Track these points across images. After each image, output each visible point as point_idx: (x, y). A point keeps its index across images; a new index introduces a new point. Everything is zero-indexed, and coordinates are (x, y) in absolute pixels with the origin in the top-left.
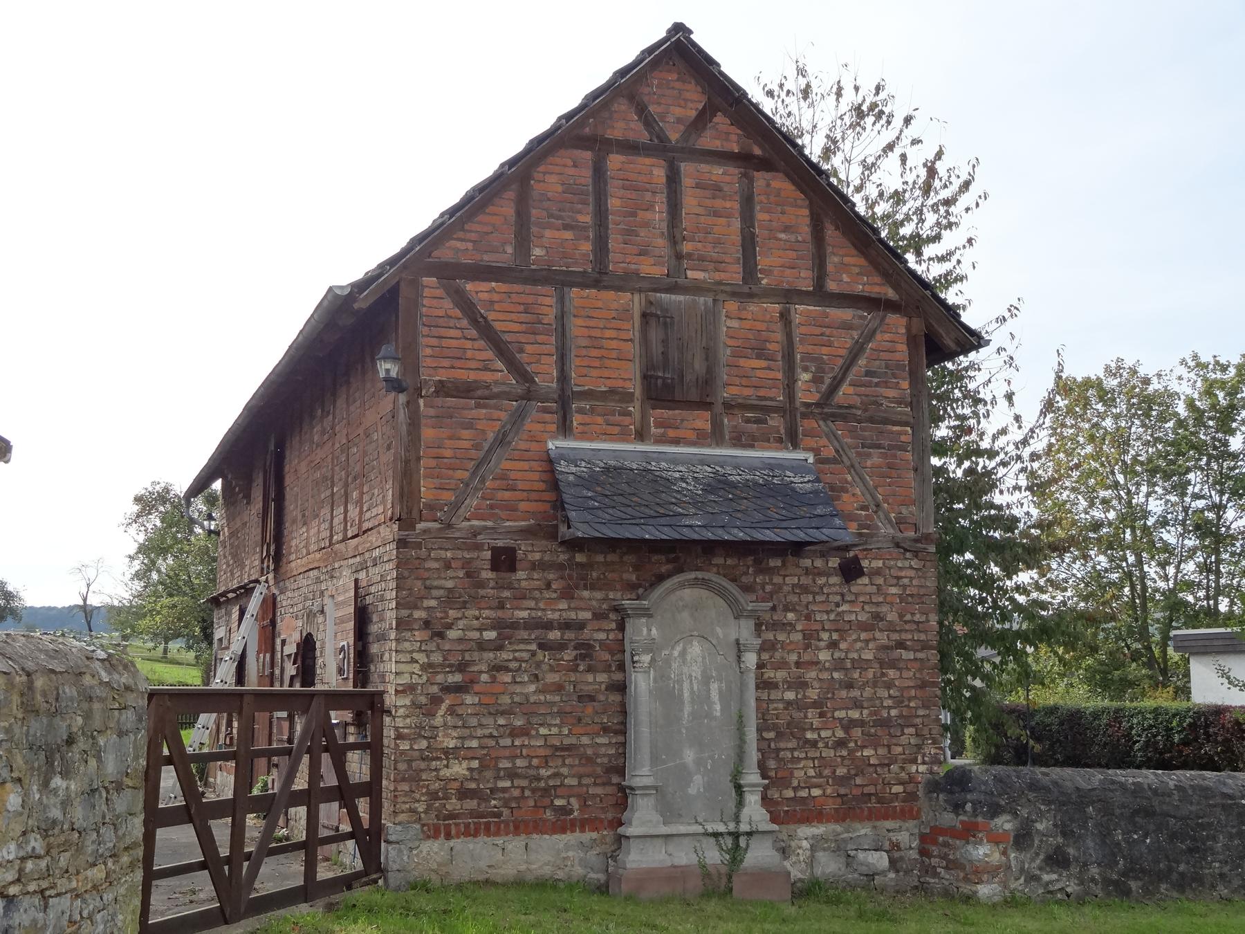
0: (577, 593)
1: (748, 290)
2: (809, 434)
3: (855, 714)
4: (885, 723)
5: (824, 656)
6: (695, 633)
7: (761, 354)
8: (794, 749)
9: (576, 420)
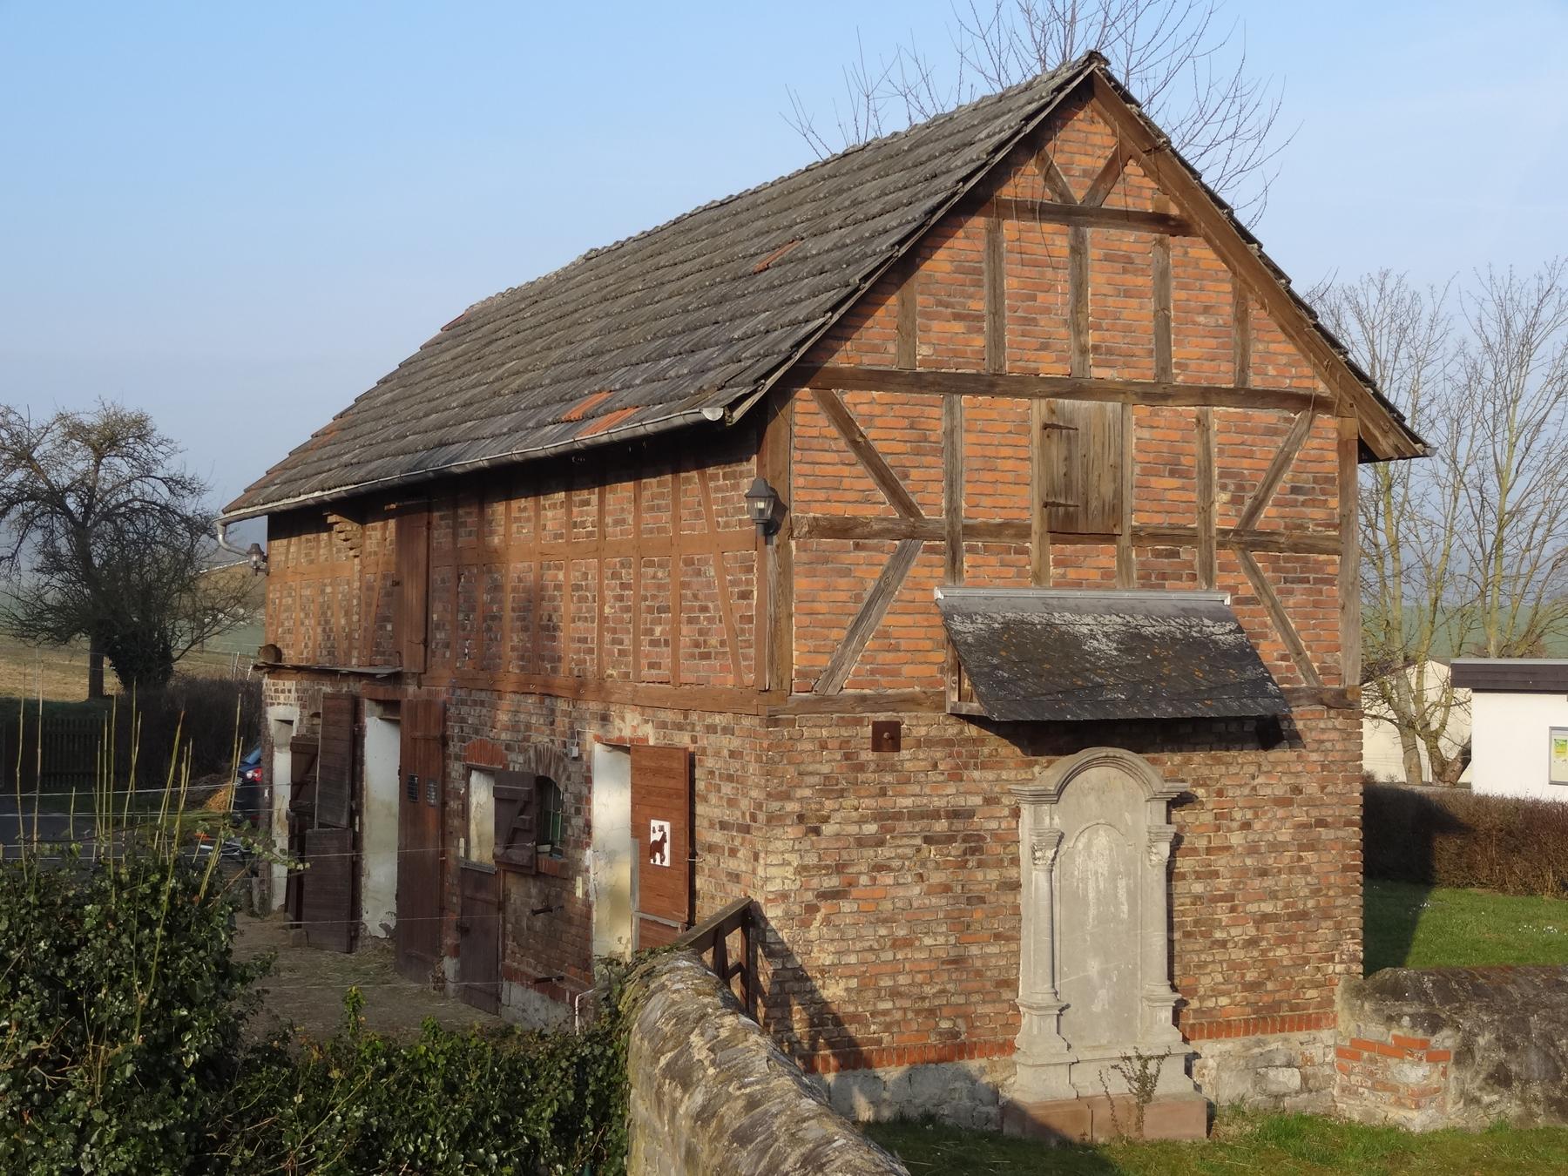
0: (966, 774)
3: (1267, 907)
4: (1304, 915)
5: (1236, 839)
6: (1102, 821)
8: (1201, 951)
9: (967, 560)
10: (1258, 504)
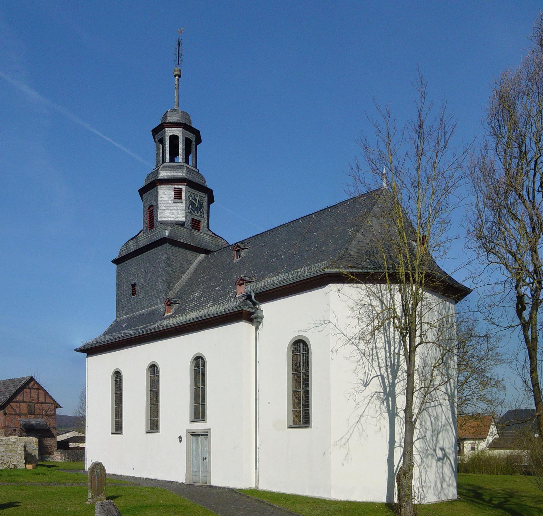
1: (38, 403)
10: (47, 412)
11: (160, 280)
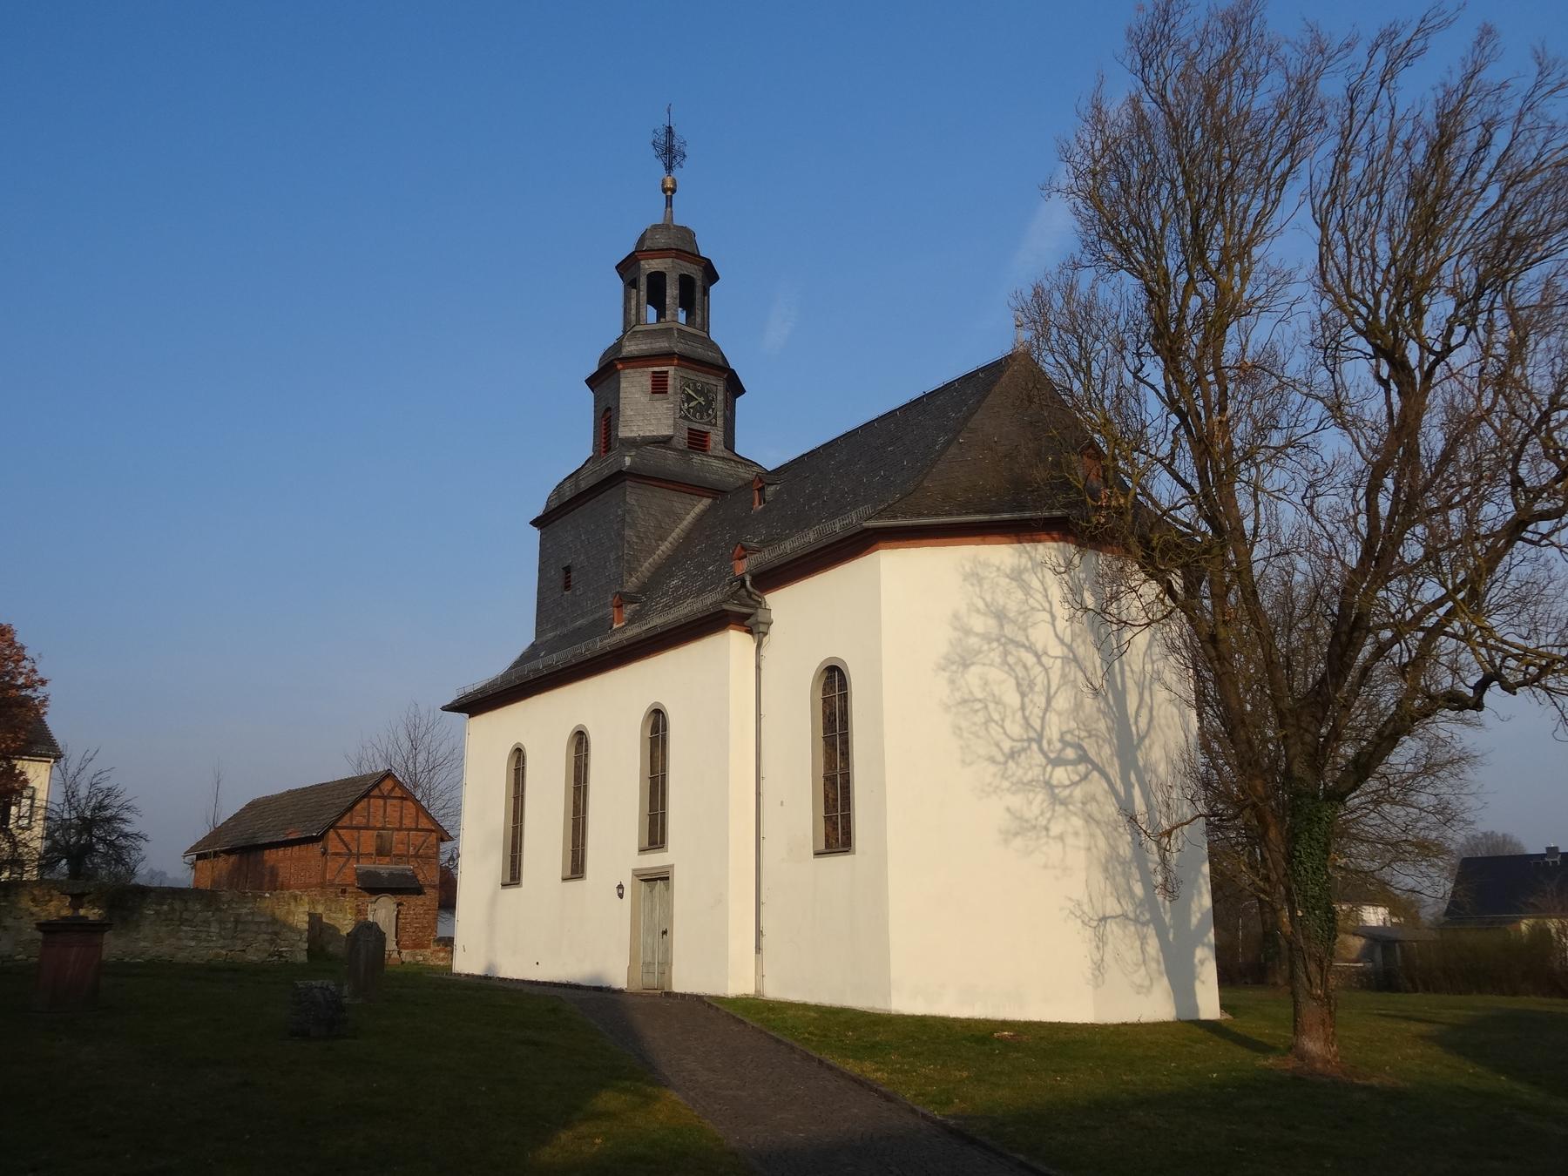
2: (412, 861)
7: (402, 844)
11: (612, 556)
